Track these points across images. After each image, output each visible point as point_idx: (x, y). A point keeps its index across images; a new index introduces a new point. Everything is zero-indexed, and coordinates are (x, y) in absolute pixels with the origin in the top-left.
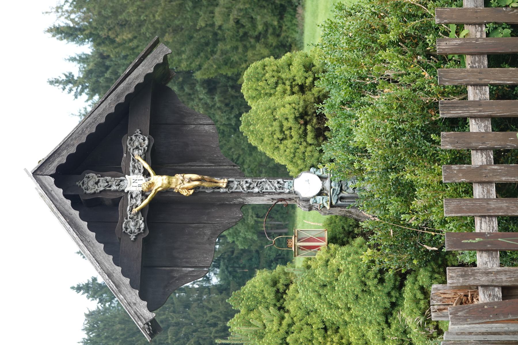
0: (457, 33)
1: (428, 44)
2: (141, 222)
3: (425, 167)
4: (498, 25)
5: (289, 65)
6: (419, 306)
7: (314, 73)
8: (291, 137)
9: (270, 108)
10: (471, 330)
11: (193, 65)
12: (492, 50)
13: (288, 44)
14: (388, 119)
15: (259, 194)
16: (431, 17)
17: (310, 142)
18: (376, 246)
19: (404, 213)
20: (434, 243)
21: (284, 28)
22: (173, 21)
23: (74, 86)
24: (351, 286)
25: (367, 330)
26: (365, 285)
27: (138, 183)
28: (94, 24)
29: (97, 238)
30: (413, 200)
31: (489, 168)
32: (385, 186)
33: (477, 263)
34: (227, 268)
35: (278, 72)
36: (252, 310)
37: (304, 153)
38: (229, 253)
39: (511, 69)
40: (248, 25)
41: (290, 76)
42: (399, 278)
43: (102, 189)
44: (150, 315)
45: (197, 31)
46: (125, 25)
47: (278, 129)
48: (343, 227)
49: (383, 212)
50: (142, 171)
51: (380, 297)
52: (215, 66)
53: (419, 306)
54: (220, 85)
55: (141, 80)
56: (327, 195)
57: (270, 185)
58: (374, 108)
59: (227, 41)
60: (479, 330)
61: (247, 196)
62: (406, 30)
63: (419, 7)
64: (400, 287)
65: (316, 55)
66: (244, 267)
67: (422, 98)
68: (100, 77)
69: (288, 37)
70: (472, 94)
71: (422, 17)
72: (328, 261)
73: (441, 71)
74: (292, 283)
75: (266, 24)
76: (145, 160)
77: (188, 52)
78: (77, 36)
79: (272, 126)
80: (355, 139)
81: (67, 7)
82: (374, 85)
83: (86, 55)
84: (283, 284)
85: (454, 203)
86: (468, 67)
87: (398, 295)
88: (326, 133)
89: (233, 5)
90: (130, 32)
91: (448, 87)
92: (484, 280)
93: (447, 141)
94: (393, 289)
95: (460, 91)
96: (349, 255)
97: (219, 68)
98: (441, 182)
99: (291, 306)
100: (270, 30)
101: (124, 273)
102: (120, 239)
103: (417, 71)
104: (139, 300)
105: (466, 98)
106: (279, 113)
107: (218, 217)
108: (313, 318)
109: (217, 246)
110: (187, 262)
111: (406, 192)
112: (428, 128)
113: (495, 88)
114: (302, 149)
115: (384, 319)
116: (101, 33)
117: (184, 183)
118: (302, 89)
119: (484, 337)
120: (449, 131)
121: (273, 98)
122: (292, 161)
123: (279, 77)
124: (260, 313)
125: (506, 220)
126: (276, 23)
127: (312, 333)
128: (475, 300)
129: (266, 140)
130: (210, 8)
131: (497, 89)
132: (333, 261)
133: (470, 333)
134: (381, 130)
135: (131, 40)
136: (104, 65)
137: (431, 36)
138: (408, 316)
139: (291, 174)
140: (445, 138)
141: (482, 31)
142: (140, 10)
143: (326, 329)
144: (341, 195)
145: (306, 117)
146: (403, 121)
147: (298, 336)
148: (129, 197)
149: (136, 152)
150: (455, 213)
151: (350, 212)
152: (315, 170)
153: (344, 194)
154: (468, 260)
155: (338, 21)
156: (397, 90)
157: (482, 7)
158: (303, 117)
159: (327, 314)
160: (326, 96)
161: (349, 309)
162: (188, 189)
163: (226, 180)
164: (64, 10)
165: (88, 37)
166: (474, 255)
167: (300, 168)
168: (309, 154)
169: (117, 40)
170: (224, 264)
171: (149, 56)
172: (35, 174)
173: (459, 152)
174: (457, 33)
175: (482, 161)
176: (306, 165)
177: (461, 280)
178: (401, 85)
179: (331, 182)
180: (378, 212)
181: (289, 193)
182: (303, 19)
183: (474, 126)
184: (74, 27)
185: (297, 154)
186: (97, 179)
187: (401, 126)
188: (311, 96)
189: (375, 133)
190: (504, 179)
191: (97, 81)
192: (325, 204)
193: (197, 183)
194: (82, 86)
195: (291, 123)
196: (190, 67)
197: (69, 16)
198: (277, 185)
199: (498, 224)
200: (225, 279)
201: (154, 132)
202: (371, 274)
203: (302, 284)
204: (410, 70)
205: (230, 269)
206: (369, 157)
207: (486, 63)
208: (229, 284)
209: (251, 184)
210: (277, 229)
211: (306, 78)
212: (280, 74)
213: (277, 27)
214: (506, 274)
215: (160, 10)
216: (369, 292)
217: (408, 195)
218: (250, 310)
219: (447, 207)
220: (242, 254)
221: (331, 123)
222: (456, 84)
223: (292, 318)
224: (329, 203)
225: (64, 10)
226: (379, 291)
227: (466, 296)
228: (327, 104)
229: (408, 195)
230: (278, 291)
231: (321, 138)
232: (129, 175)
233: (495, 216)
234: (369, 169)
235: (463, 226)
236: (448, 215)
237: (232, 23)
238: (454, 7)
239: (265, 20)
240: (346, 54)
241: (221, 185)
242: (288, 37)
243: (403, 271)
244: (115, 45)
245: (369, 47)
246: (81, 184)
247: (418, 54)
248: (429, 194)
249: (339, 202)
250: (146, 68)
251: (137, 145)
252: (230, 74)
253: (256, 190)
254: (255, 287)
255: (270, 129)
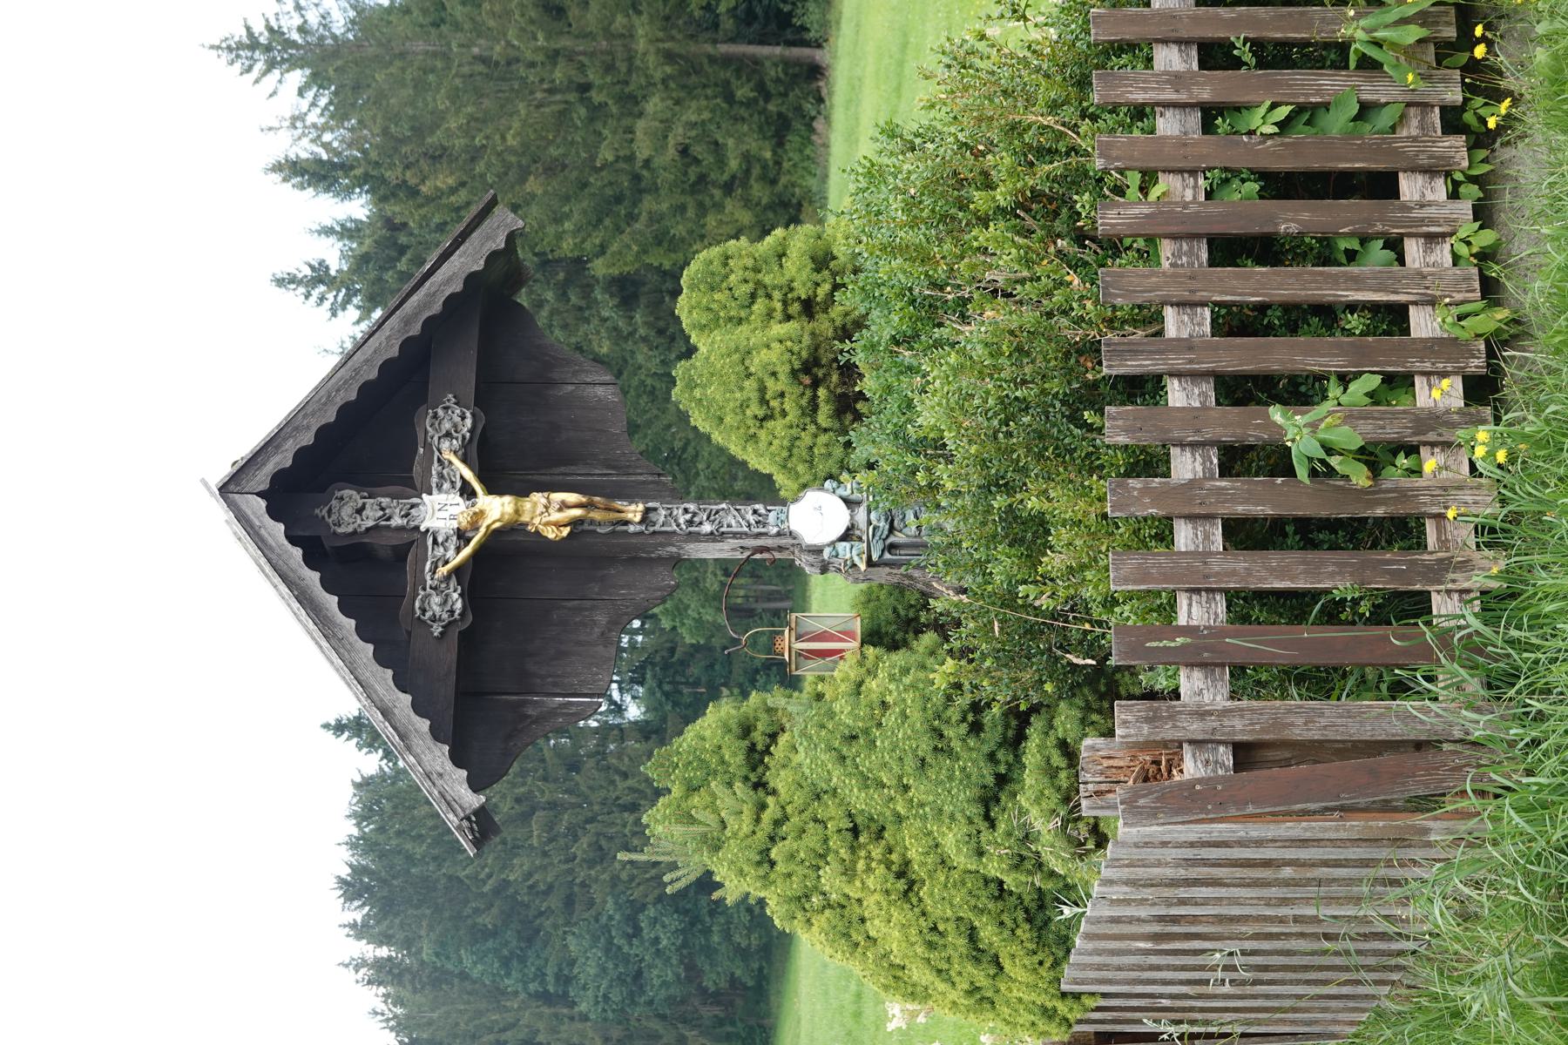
0: (1144, 190)
1: (1079, 214)
2: (455, 596)
3: (1071, 481)
4: (1231, 174)
5: (781, 256)
6: (1057, 782)
7: (834, 274)
8: (784, 414)
9: (737, 350)
10: (1167, 838)
11: (588, 245)
12: (1217, 229)
13: (794, 201)
14: (991, 376)
15: (712, 537)
16: (1088, 155)
17: (824, 425)
18: (964, 653)
19: (1025, 582)
20: (1091, 645)
21: (786, 165)
22: (546, 148)
23: (330, 290)
24: (909, 738)
25: (944, 834)
26: (941, 736)
27: (450, 511)
28: (374, 155)
29: (360, 631)
30: (1045, 554)
31: (1208, 484)
32: (984, 524)
33: (1182, 691)
34: (660, 686)
35: (757, 270)
36: (697, 789)
37: (811, 448)
38: (665, 654)
39: (1258, 269)
40: (708, 159)
41: (782, 281)
42: (1014, 723)
43: (370, 523)
44: (473, 800)
45: (598, 170)
46: (440, 156)
47: (754, 396)
48: (895, 610)
49: (979, 579)
50: (459, 485)
51: (972, 763)
52: (635, 248)
53: (1057, 782)
54: (646, 289)
55: (457, 287)
56: (860, 539)
57: (737, 518)
58: (963, 352)
59: (662, 192)
60: (1183, 838)
61: (686, 541)
62: (1031, 183)
63: (1062, 133)
64: (1015, 741)
65: (839, 235)
66: (696, 684)
67: (1066, 332)
68: (387, 270)
69: (793, 185)
70: (1174, 324)
71: (1068, 154)
72: (860, 684)
73: (1107, 274)
74: (783, 730)
75: (747, 158)
76: (464, 460)
77: (576, 216)
78: (336, 181)
79: (742, 389)
80: (920, 420)
81: (314, 117)
82: (964, 302)
83: (355, 221)
84: (763, 734)
85: (1133, 562)
86: (1166, 264)
87: (1011, 758)
88: (859, 406)
89: (674, 115)
90: (452, 173)
91: (1122, 308)
92: (1195, 728)
93: (1118, 427)
94: (1000, 745)
95: (1149, 318)
96: (905, 671)
97: (645, 252)
98: (1105, 516)
99: (781, 781)
100: (756, 171)
101: (417, 708)
102: (409, 633)
103: (1055, 272)
104: (449, 766)
105: (1160, 333)
106: (756, 361)
107: (622, 587)
108: (827, 806)
109: (640, 638)
110: (555, 684)
111: (1030, 535)
112: (1078, 398)
113: (1223, 311)
114: (807, 439)
115: (982, 811)
116: (387, 174)
117: (549, 513)
118: (809, 308)
119: (1195, 851)
120: (1123, 404)
121: (744, 328)
122: (784, 467)
123: (758, 283)
124: (714, 796)
125: (1245, 599)
126: (768, 155)
127: (826, 841)
128: (1175, 772)
129: (728, 419)
130: (627, 122)
131: (1229, 313)
132: (872, 684)
133: (1164, 844)
134: (977, 402)
135: (453, 191)
136: (395, 243)
137: (1086, 196)
138: (1032, 806)
139: (782, 493)
140: (1114, 419)
141: (1196, 186)
142: (473, 124)
143: (855, 831)
144: (892, 539)
145: (815, 370)
146: (1024, 382)
147: (795, 846)
148: (430, 541)
149: (445, 445)
150: (1135, 582)
151: (911, 577)
152: (835, 484)
153: (899, 538)
154: (1162, 683)
155: (886, 161)
156: (1011, 313)
157: (1197, 135)
158: (809, 369)
159: (859, 800)
160: (859, 324)
161: (906, 788)
162: (559, 525)
163: (641, 507)
164: (308, 123)
165: (361, 181)
166: (1175, 675)
167: (802, 480)
168: (823, 451)
169: (424, 189)
170: (654, 676)
171: (474, 235)
172: (224, 490)
173: (1143, 450)
174: (1144, 190)
175: (1194, 472)
176: (815, 475)
177: (1146, 729)
178: (1021, 303)
179: (869, 512)
180: (969, 578)
181: (779, 534)
182: (826, 146)
183: (1177, 395)
184: (330, 162)
185: (795, 451)
186: (360, 502)
187: (1018, 394)
188: (827, 324)
189: (962, 407)
190: (1240, 509)
191: (380, 279)
192: (856, 559)
193: (577, 512)
194: (348, 289)
195: (783, 382)
196: (583, 250)
197: (319, 137)
198: (751, 518)
199: (1228, 607)
200: (655, 709)
201: (483, 401)
202: (954, 713)
203: (803, 734)
204: (1038, 270)
205: (667, 687)
206: (949, 459)
207: (1204, 256)
208: (664, 719)
209: (695, 514)
210: (769, 600)
211: (817, 284)
212: (760, 276)
213: (771, 163)
214: (1242, 717)
215: (516, 125)
216: (950, 753)
217: (1034, 542)
218: (692, 789)
219: (1116, 570)
220: (692, 655)
221: (869, 384)
222: (1139, 302)
223: (783, 807)
224: (865, 557)
225: (308, 123)
226: (971, 749)
227: (1157, 763)
228: (863, 342)
229: (1034, 542)
230: (752, 748)
231: (849, 417)
232: (430, 493)
233: (1220, 590)
234: (949, 486)
235: (1151, 610)
236: (1119, 588)
237: (671, 152)
238: (1136, 133)
239: (744, 148)
240: (902, 234)
241: (630, 516)
242: (793, 185)
243: (1023, 708)
244: (420, 200)
245: (953, 218)
246: (324, 512)
247: (1059, 236)
248: (1079, 542)
249: (887, 556)
250: (469, 259)
251: (448, 428)
252: (667, 265)
253: (707, 528)
254: (703, 739)
255: (738, 395)
